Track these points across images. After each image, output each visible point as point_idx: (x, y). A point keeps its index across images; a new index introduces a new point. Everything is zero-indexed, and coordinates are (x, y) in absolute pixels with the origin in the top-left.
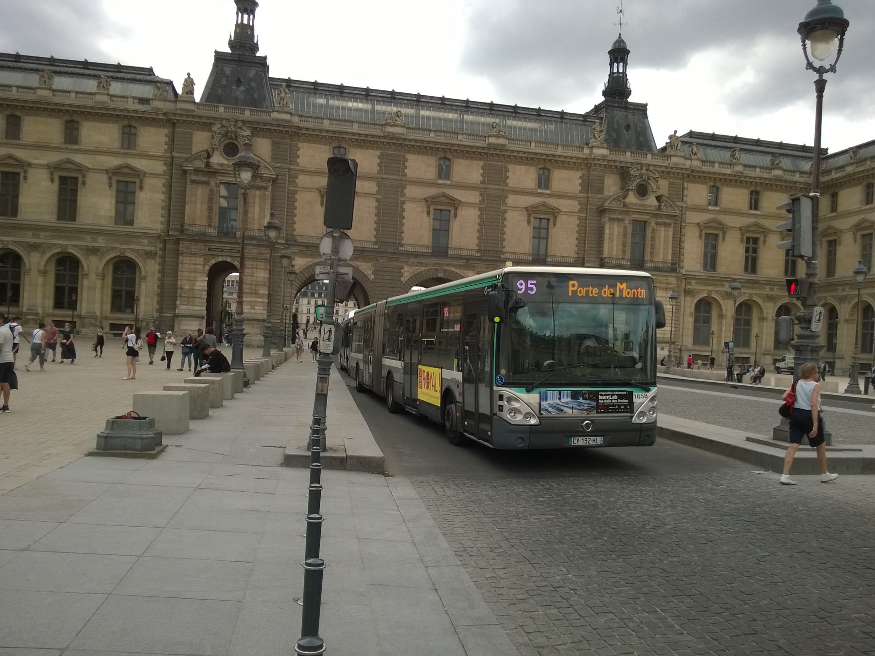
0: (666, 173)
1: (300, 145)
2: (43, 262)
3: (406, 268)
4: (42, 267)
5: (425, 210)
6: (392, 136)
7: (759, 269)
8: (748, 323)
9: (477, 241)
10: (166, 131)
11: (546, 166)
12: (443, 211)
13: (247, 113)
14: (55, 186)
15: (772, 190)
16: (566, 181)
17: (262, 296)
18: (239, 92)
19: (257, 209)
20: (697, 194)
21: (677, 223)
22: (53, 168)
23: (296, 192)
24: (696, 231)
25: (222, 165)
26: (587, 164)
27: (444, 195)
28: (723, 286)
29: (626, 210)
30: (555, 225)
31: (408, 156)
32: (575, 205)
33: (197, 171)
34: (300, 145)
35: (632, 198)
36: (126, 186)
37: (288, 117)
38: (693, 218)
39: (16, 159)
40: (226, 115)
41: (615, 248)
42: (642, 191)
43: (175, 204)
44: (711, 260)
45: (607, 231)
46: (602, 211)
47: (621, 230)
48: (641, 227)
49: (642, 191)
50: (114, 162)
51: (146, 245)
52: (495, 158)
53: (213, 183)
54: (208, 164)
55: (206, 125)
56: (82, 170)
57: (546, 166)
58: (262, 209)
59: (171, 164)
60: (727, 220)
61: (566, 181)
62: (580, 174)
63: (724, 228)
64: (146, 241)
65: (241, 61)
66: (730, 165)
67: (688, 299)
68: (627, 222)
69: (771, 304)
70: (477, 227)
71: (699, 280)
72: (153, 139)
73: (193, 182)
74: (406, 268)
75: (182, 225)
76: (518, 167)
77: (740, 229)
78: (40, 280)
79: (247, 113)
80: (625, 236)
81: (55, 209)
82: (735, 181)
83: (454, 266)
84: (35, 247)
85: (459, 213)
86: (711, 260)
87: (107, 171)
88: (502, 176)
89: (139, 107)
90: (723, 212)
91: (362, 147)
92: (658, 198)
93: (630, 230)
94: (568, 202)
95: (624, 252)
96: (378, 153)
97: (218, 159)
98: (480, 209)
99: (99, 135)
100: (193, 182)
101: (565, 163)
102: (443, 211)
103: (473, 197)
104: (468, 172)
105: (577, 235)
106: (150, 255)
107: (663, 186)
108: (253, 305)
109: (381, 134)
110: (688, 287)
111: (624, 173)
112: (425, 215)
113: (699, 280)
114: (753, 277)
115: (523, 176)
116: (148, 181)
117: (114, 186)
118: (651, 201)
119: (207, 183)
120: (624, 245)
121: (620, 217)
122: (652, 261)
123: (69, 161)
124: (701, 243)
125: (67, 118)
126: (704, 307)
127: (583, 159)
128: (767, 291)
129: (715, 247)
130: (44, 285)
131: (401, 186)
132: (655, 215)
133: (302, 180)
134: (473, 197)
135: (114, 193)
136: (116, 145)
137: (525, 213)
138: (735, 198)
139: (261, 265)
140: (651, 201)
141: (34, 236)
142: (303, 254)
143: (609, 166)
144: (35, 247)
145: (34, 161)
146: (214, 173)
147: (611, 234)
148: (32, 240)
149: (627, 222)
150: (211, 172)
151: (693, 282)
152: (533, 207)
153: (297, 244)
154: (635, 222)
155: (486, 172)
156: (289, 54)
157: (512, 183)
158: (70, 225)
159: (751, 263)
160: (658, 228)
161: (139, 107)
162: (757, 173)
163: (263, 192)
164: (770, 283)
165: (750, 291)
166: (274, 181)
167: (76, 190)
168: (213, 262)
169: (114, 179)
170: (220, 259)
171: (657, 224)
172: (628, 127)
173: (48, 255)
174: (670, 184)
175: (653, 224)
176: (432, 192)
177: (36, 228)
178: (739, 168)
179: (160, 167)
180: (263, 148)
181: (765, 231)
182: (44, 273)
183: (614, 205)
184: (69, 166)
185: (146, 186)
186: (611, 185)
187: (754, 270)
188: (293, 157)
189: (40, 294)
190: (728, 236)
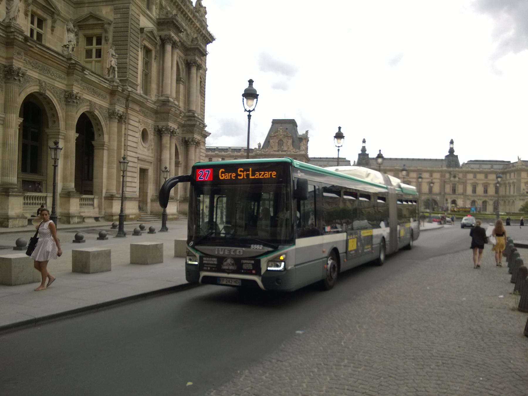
0: (461, 172)
6: (396, 169)
8: (486, 206)
11: (431, 173)
16: (437, 175)
20: (470, 176)
21: (465, 184)
26: (441, 172)
29: (451, 181)
35: (452, 179)
38: (469, 182)
42: (455, 177)
44: (474, 191)
46: (445, 182)
49: (455, 177)
52: (420, 172)
57: (431, 173)
61: (437, 175)
63: (477, 184)
82: (480, 172)
86: (474, 191)
90: (477, 180)
92: (459, 178)
101: (436, 172)
107: (461, 175)
111: (450, 173)
115: (426, 175)
118: (457, 179)
128: (490, 198)
129: (475, 188)
138: (481, 176)
143: (446, 172)
154: (453, 184)
159: (486, 191)
162: (487, 170)
164: (491, 196)
178: (481, 169)
181: (489, 184)
183: (447, 180)
186: (447, 176)
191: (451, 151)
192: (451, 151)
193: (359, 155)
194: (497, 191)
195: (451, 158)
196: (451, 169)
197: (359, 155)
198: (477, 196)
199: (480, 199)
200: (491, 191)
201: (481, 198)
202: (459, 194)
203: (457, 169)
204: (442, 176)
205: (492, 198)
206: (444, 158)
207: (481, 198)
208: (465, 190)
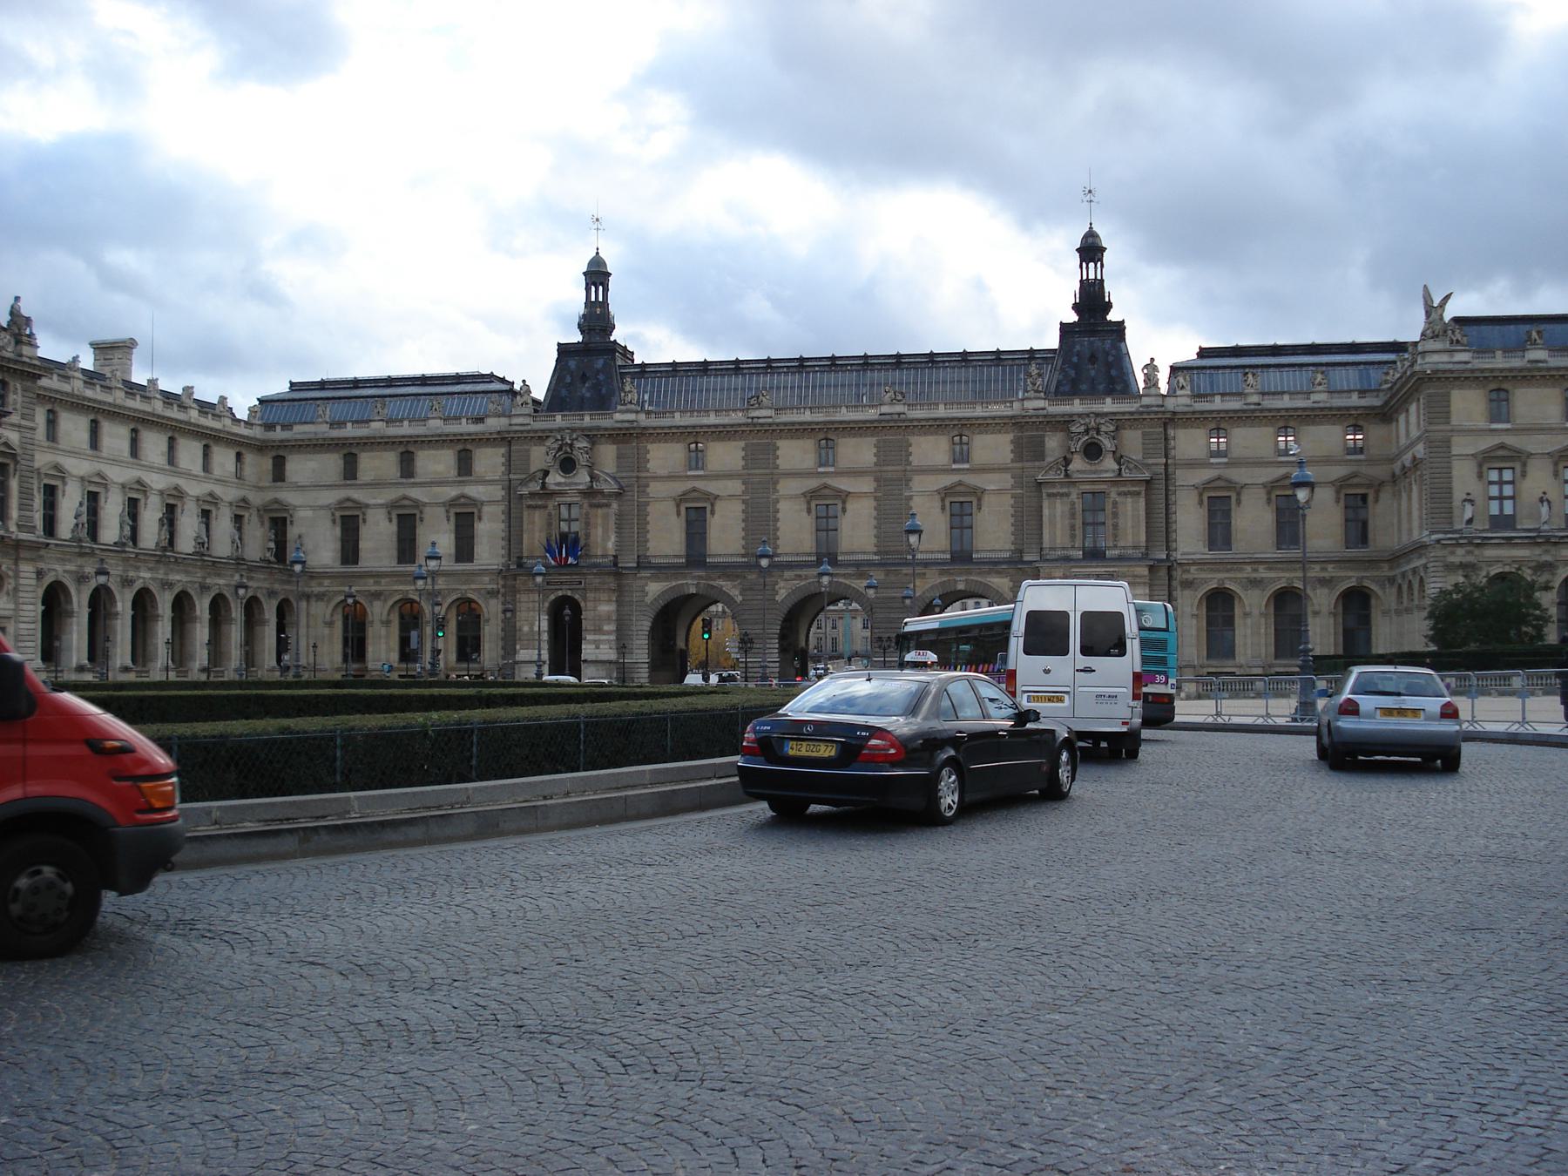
1: (650, 447)
2: (329, 611)
3: (782, 584)
4: (384, 618)
5: (805, 506)
7: (1371, 542)
9: (874, 540)
10: (503, 450)
12: (825, 505)
13: (587, 418)
14: (394, 527)
15: (1313, 423)
17: (608, 633)
18: (585, 391)
19: (600, 530)
21: (1157, 490)
22: (391, 506)
23: (647, 504)
24: (1194, 494)
25: (559, 484)
27: (826, 487)
28: (1241, 570)
30: (979, 509)
31: (780, 443)
32: (1006, 480)
33: (532, 495)
34: (650, 447)
35: (1078, 464)
36: (465, 522)
37: (632, 417)
38: (1185, 478)
39: (354, 501)
40: (564, 424)
41: (1058, 533)
42: (1093, 451)
43: (513, 536)
45: (1046, 512)
47: (1067, 508)
48: (1095, 502)
49: (1093, 451)
50: (452, 492)
51: (487, 583)
53: (550, 507)
54: (544, 485)
55: (541, 437)
56: (417, 504)
58: (605, 531)
59: (509, 488)
60: (1239, 475)
61: (994, 448)
62: (1010, 437)
64: (487, 579)
65: (592, 360)
66: (1241, 394)
67: (1187, 592)
68: (1074, 496)
69: (1257, 592)
70: (874, 522)
71: (1271, 564)
72: (489, 461)
73: (529, 507)
74: (782, 584)
75: (520, 558)
76: (922, 439)
77: (1264, 485)
78: (383, 631)
79: (587, 418)
80: (1073, 516)
81: (395, 553)
83: (844, 575)
84: (377, 595)
85: (849, 506)
87: (444, 504)
88: (904, 452)
89: (473, 428)
91: (723, 440)
93: (1079, 507)
94: (995, 476)
95: (1073, 537)
96: (742, 444)
97: (555, 478)
98: (876, 498)
99: (436, 464)
100: (529, 507)
102: (825, 505)
103: (736, 487)
104: (859, 452)
105: (1012, 520)
106: (492, 594)
108: (597, 644)
109: (744, 420)
110: (1185, 576)
112: (805, 514)
113: (1271, 564)
114: (1294, 553)
116: (486, 509)
117: (453, 519)
118: (1109, 463)
119: (545, 507)
120: (1073, 528)
121: (1065, 490)
122: (1115, 547)
123: (405, 498)
124: (1204, 512)
125: (460, 447)
126: (1220, 604)
127: (1012, 417)
130: (387, 636)
131: (772, 481)
132: (1114, 483)
133: (655, 489)
134: (866, 485)
135: (452, 527)
136: (453, 473)
137: (937, 497)
139: (604, 596)
140: (1109, 463)
141: (376, 583)
142: (655, 578)
144: (377, 595)
145: (372, 502)
146: (553, 494)
147: (1052, 517)
148: (373, 588)
149: (1074, 496)
150: (546, 494)
151: (1193, 569)
152: (946, 489)
153: (650, 566)
155: (880, 450)
156: (650, 339)
157: (915, 460)
158: (352, 569)
160: (594, 511)
161: (473, 428)
163: (605, 510)
165: (1287, 575)
166: (618, 495)
167: (415, 527)
168: (552, 597)
169: (453, 511)
170: (560, 593)
171: (591, 506)
172: (1093, 358)
173: (390, 603)
174: (1144, 434)
175: (1113, 495)
176: (813, 483)
177: (377, 576)
179: (498, 492)
180: (608, 454)
182: (387, 623)
183: (1051, 476)
184: (406, 502)
185: (485, 518)
187: (1227, 543)
188: (641, 462)
189: (383, 647)
190: (1244, 498)
191: (1092, 300)
192: (1092, 300)
193: (564, 350)
194: (1358, 531)
195: (1083, 344)
196: (1077, 406)
197: (564, 350)
198: (1236, 564)
199: (1255, 583)
200: (1324, 524)
201: (1263, 573)
202: (1120, 558)
203: (1109, 405)
204: (1028, 446)
205: (1331, 571)
206: (1052, 341)
207: (1263, 573)
208: (1161, 526)
